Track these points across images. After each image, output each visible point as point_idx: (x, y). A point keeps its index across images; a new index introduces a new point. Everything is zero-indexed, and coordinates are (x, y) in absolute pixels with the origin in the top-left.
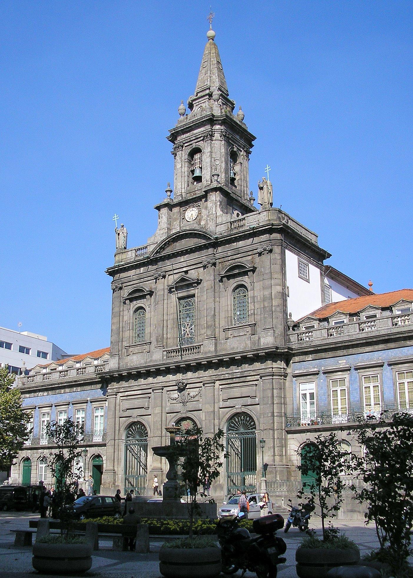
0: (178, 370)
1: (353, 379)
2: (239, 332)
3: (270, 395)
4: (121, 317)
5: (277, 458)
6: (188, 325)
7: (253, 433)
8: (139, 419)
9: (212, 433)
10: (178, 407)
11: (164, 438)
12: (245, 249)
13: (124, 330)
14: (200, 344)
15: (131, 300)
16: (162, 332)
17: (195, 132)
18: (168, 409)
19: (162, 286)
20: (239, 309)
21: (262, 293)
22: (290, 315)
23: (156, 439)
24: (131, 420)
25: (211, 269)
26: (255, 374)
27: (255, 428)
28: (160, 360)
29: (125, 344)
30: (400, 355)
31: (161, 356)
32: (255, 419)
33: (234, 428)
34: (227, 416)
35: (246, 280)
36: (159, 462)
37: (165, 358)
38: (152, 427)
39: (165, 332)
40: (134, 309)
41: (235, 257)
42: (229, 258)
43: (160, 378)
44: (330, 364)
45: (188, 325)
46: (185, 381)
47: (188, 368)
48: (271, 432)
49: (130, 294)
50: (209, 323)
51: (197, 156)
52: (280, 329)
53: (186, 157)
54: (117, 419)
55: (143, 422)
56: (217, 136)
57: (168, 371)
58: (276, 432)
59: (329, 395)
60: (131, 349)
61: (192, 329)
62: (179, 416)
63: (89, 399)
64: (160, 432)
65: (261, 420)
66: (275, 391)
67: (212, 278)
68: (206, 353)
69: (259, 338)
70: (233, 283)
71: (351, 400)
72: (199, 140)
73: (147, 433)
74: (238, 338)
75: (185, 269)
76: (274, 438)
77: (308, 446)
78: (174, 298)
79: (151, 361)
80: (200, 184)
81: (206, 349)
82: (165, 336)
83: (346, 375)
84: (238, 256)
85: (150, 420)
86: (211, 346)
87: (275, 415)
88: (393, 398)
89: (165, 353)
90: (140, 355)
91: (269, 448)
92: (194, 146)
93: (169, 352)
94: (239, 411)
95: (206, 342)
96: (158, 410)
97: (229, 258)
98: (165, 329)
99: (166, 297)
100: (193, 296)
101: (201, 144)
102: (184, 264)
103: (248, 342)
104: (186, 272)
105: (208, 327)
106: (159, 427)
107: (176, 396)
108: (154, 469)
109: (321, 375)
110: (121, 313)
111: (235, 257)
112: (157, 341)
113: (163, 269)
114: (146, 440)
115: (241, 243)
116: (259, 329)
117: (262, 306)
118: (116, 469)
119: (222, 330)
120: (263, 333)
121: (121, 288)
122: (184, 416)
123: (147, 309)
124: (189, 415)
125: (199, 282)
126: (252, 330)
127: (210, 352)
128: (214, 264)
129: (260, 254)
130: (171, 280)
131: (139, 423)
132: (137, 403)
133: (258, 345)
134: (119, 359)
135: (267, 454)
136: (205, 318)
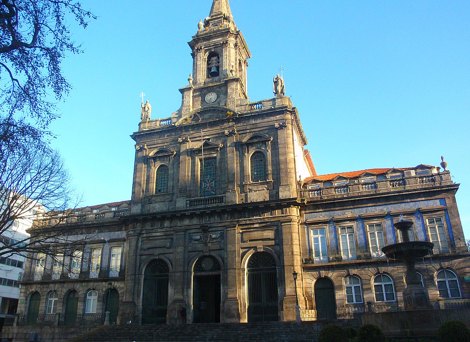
0: (202, 215)
3: (290, 237)
6: (208, 181)
7: (275, 268)
8: (162, 257)
10: (200, 246)
14: (223, 195)
17: (214, 40)
20: (255, 170)
22: (300, 177)
23: (179, 274)
24: (152, 258)
27: (275, 265)
32: (276, 256)
33: (253, 264)
37: (188, 206)
38: (174, 264)
41: (253, 130)
42: (248, 131)
44: (338, 214)
45: (208, 181)
46: (209, 225)
47: (213, 213)
48: (292, 267)
51: (214, 58)
54: (138, 257)
55: (165, 259)
57: (192, 216)
61: (212, 184)
62: (201, 254)
63: (106, 240)
72: (217, 46)
73: (168, 268)
75: (207, 137)
79: (173, 208)
80: (217, 77)
83: (354, 224)
84: (256, 130)
85: (171, 258)
89: (188, 202)
91: (291, 282)
92: (213, 50)
93: (191, 201)
96: (180, 249)
97: (248, 131)
100: (215, 158)
104: (209, 139)
107: (198, 237)
108: (176, 301)
111: (253, 130)
112: (180, 192)
115: (259, 121)
118: (136, 301)
131: (161, 261)
132: (158, 243)
134: (142, 206)
135: (289, 287)
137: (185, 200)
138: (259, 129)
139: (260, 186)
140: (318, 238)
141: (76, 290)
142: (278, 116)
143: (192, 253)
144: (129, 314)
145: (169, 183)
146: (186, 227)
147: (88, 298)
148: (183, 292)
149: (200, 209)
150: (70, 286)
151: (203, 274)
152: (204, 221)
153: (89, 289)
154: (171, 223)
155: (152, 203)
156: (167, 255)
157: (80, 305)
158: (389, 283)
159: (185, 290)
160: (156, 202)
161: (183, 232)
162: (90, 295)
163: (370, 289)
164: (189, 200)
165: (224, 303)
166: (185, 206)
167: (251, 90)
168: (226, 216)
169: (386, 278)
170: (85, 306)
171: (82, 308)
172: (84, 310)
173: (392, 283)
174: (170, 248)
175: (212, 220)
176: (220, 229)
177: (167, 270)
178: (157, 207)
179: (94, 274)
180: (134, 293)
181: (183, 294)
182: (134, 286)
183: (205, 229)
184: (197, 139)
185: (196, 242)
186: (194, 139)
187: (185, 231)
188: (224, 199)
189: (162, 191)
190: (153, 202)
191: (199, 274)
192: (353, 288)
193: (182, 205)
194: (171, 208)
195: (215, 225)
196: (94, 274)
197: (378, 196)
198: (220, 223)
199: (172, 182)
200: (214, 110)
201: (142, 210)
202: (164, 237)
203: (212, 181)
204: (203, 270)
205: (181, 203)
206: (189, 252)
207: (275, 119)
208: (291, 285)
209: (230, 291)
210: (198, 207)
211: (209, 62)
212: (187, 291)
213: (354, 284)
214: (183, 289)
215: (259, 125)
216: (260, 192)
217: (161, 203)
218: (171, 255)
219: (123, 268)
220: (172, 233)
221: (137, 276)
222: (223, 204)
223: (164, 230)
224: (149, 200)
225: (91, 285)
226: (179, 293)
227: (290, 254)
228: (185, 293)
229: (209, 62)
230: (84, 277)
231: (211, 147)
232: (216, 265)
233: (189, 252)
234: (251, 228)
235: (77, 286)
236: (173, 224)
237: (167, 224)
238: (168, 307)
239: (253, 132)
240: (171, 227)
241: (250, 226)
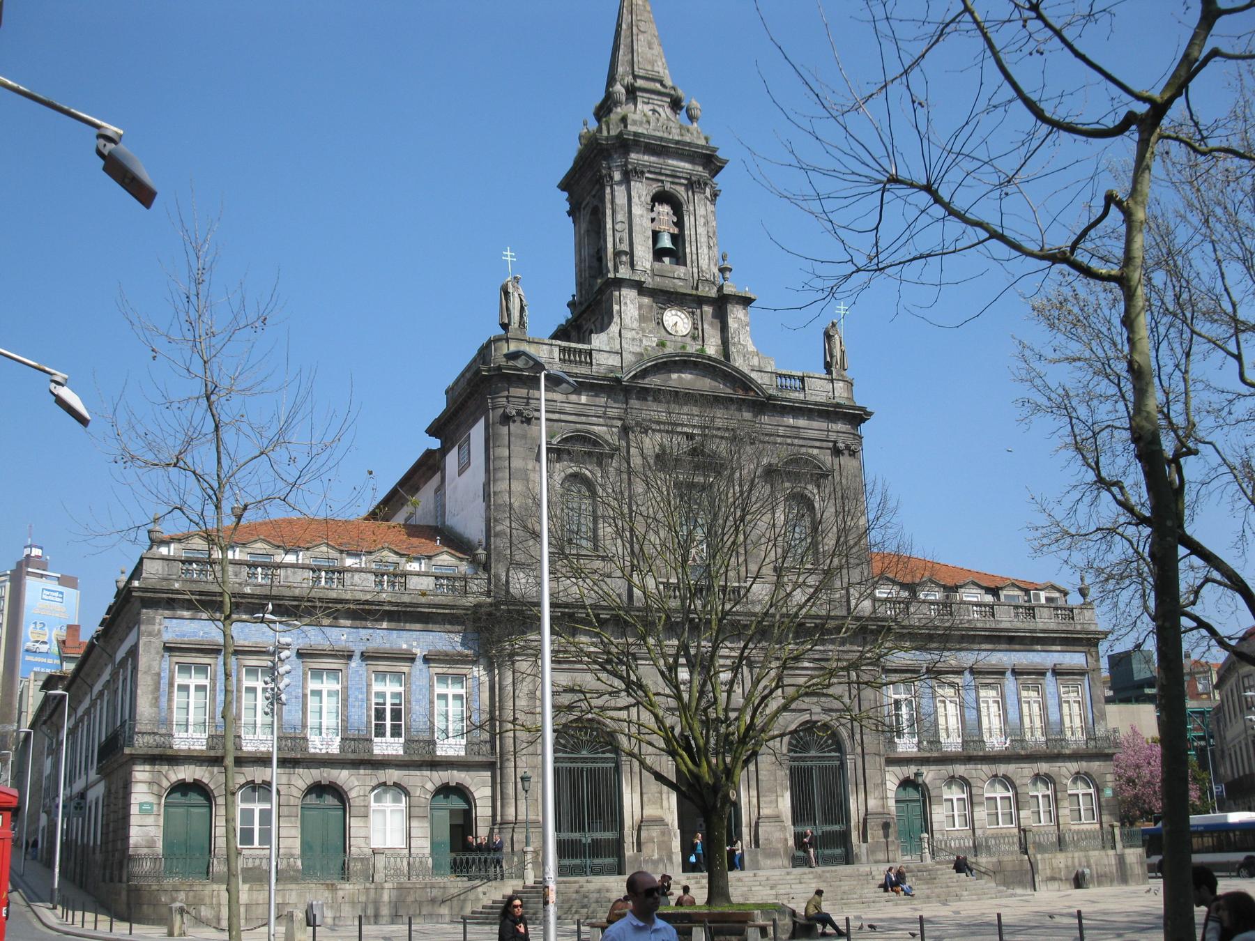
12: (810, 434)
72: (677, 180)
75: (689, 430)
84: (796, 441)
92: (668, 186)
115: (801, 422)
138: (801, 442)
215: (803, 433)
228: (665, 803)
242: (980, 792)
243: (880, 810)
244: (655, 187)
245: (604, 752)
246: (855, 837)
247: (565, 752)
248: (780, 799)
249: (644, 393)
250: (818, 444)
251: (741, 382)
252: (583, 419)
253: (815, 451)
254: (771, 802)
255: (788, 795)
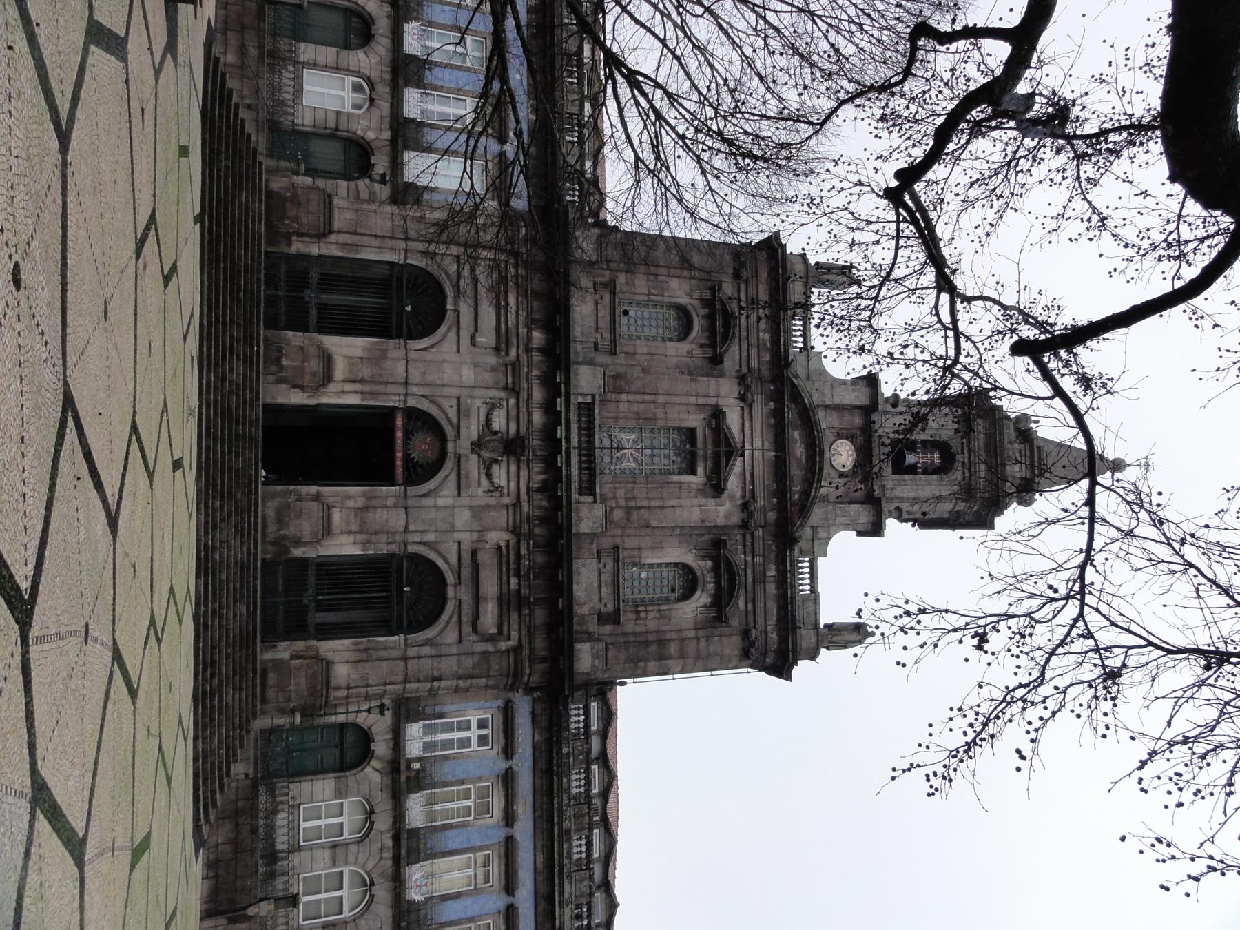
1: (489, 831)
2: (607, 586)
4: (678, 272)
5: (343, 693)
9: (406, 527)
11: (401, 390)
13: (652, 278)
15: (709, 303)
16: (633, 388)
18: (466, 402)
19: (725, 392)
21: (674, 636)
22: (623, 684)
24: (450, 292)
25: (736, 519)
26: (523, 632)
28: (576, 386)
29: (622, 278)
30: (521, 918)
31: (585, 391)
32: (430, 633)
34: (440, 563)
35: (701, 599)
36: (348, 376)
37: (580, 399)
38: (429, 356)
39: (631, 397)
40: (689, 307)
41: (749, 571)
43: (538, 394)
48: (400, 678)
49: (723, 303)
50: (635, 515)
52: (600, 676)
53: (944, 438)
55: (443, 329)
56: (961, 506)
57: (549, 408)
58: (399, 687)
59: (462, 783)
60: (607, 296)
62: (449, 431)
64: (417, 380)
65: (426, 650)
66: (484, 680)
67: (721, 521)
68: (577, 510)
69: (590, 637)
70: (702, 566)
71: (450, 833)
74: (596, 585)
76: (385, 684)
77: (365, 737)
78: (695, 420)
81: (584, 511)
82: (624, 397)
86: (591, 524)
87: (436, 684)
88: (444, 919)
89: (589, 400)
90: (593, 324)
92: (959, 458)
93: (590, 407)
94: (450, 592)
95: (598, 510)
96: (468, 375)
97: (749, 559)
98: (638, 397)
99: (701, 401)
101: (957, 475)
102: (757, 454)
103: (585, 610)
104: (743, 455)
105: (628, 510)
106: (429, 378)
109: (504, 765)
110: (686, 273)
111: (749, 571)
112: (617, 377)
113: (758, 398)
114: (399, 336)
115: (772, 588)
116: (607, 629)
117: (651, 638)
118: (333, 238)
119: (618, 541)
120: (600, 646)
121: (737, 276)
122: (450, 446)
123: (684, 347)
124: (449, 464)
125: (716, 487)
126: (608, 614)
127: (580, 520)
128: (744, 525)
129: (745, 634)
130: (733, 420)
133: (578, 632)
136: (645, 503)
137: (596, 391)
139: (610, 590)
140: (469, 729)
141: (373, 44)
142: (774, 636)
143: (455, 408)
144: (297, 219)
145: (644, 343)
146: (524, 395)
147: (350, 80)
148: (354, 381)
149: (568, 464)
150: (382, 25)
151: (399, 434)
152: (535, 442)
153: (372, 86)
154: (539, 350)
155: (596, 291)
156: (452, 335)
157: (327, 54)
158: (345, 908)
159: (358, 387)
160: (597, 304)
161: (514, 383)
162: (357, 88)
163: (334, 864)
164: (593, 403)
165: (317, 497)
166: (580, 391)
167: (851, 570)
168: (545, 503)
169: (359, 897)
170: (325, 68)
171: (321, 59)
172: (314, 65)
173: (346, 914)
174: (473, 342)
175: (537, 467)
176: (513, 484)
177: (411, 336)
178: (584, 307)
179: (414, 103)
180: (355, 233)
181: (345, 381)
182: (376, 236)
183: (513, 447)
184: (747, 424)
185: (482, 419)
186: (746, 415)
187: (517, 393)
188: (590, 499)
189: (624, 320)
190: (597, 296)
191: (399, 422)
192: (339, 820)
193: (583, 383)
194: (579, 347)
195: (524, 474)
196: (414, 103)
197: (557, 881)
198: (528, 489)
199: (645, 350)
200: (814, 473)
201: (581, 263)
202: (503, 326)
203: (635, 460)
204: (408, 435)
205: (586, 380)
206: (459, 398)
207: (769, 628)
208: (354, 677)
209: (348, 516)
210: (574, 461)
211: (929, 446)
212: (356, 392)
213: (350, 821)
214: (361, 381)
215: (759, 589)
216: (597, 592)
217: (593, 318)
218: (455, 347)
219: (426, 196)
220: (513, 352)
221: (402, 244)
222: (575, 496)
223: (523, 331)
224: (605, 285)
225: (383, 90)
226: (351, 371)
227: (436, 674)
229: (929, 446)
230: (406, 71)
231: (723, 464)
232: (419, 470)
233: (459, 398)
234: (508, 569)
235: (382, 45)
236: (537, 357)
237: (538, 336)
238: (315, 335)
239: (745, 569)
240: (528, 350)
241: (512, 566)
242: (351, 858)
243: (333, 684)
244: (955, 443)
245: (408, 326)
246: (300, 645)
247: (408, 281)
248: (351, 538)
249: (777, 397)
250: (750, 607)
251: (804, 510)
252: (744, 334)
253: (741, 605)
254: (348, 523)
255: (356, 551)
